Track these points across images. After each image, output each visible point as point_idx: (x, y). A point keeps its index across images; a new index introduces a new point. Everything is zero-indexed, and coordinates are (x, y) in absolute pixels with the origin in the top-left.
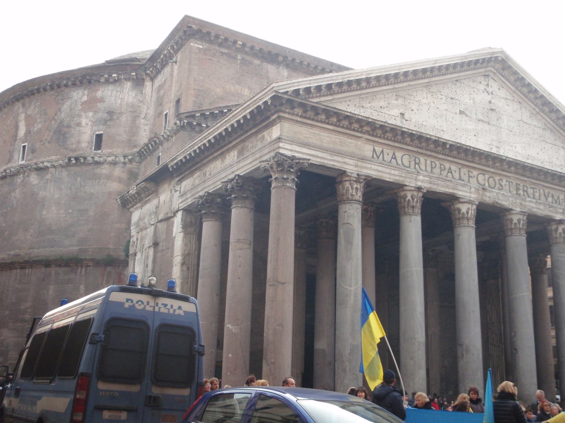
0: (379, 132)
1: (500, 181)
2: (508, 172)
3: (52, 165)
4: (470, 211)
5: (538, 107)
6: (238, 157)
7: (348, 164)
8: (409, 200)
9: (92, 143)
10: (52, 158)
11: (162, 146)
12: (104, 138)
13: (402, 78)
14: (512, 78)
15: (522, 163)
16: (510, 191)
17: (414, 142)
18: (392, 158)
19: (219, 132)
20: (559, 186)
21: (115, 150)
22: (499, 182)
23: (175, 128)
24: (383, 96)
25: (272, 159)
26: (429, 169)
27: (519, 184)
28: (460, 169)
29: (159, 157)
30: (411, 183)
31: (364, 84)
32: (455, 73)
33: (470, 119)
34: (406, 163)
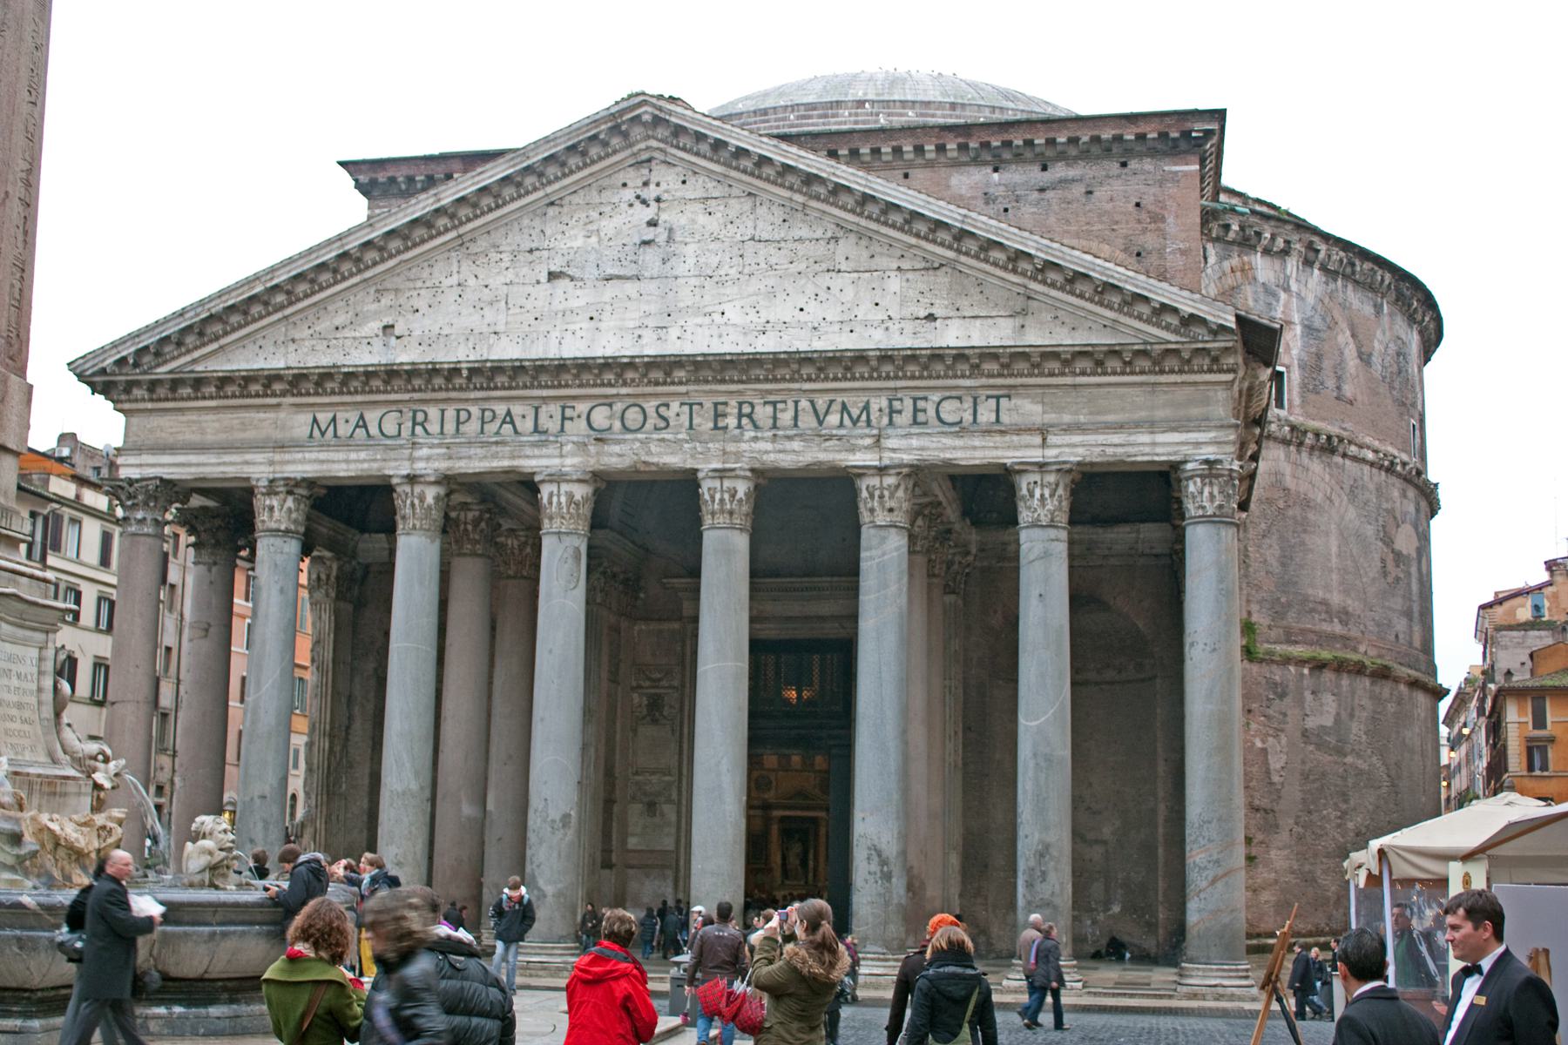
1: (662, 410)
2: (673, 383)
4: (555, 499)
5: (800, 192)
7: (254, 464)
14: (704, 148)
16: (691, 427)
18: (357, 426)
20: (854, 379)
22: (657, 412)
24: (342, 304)
26: (450, 427)
27: (726, 404)
28: (537, 409)
30: (397, 469)
32: (528, 193)
33: (581, 283)
34: (390, 427)
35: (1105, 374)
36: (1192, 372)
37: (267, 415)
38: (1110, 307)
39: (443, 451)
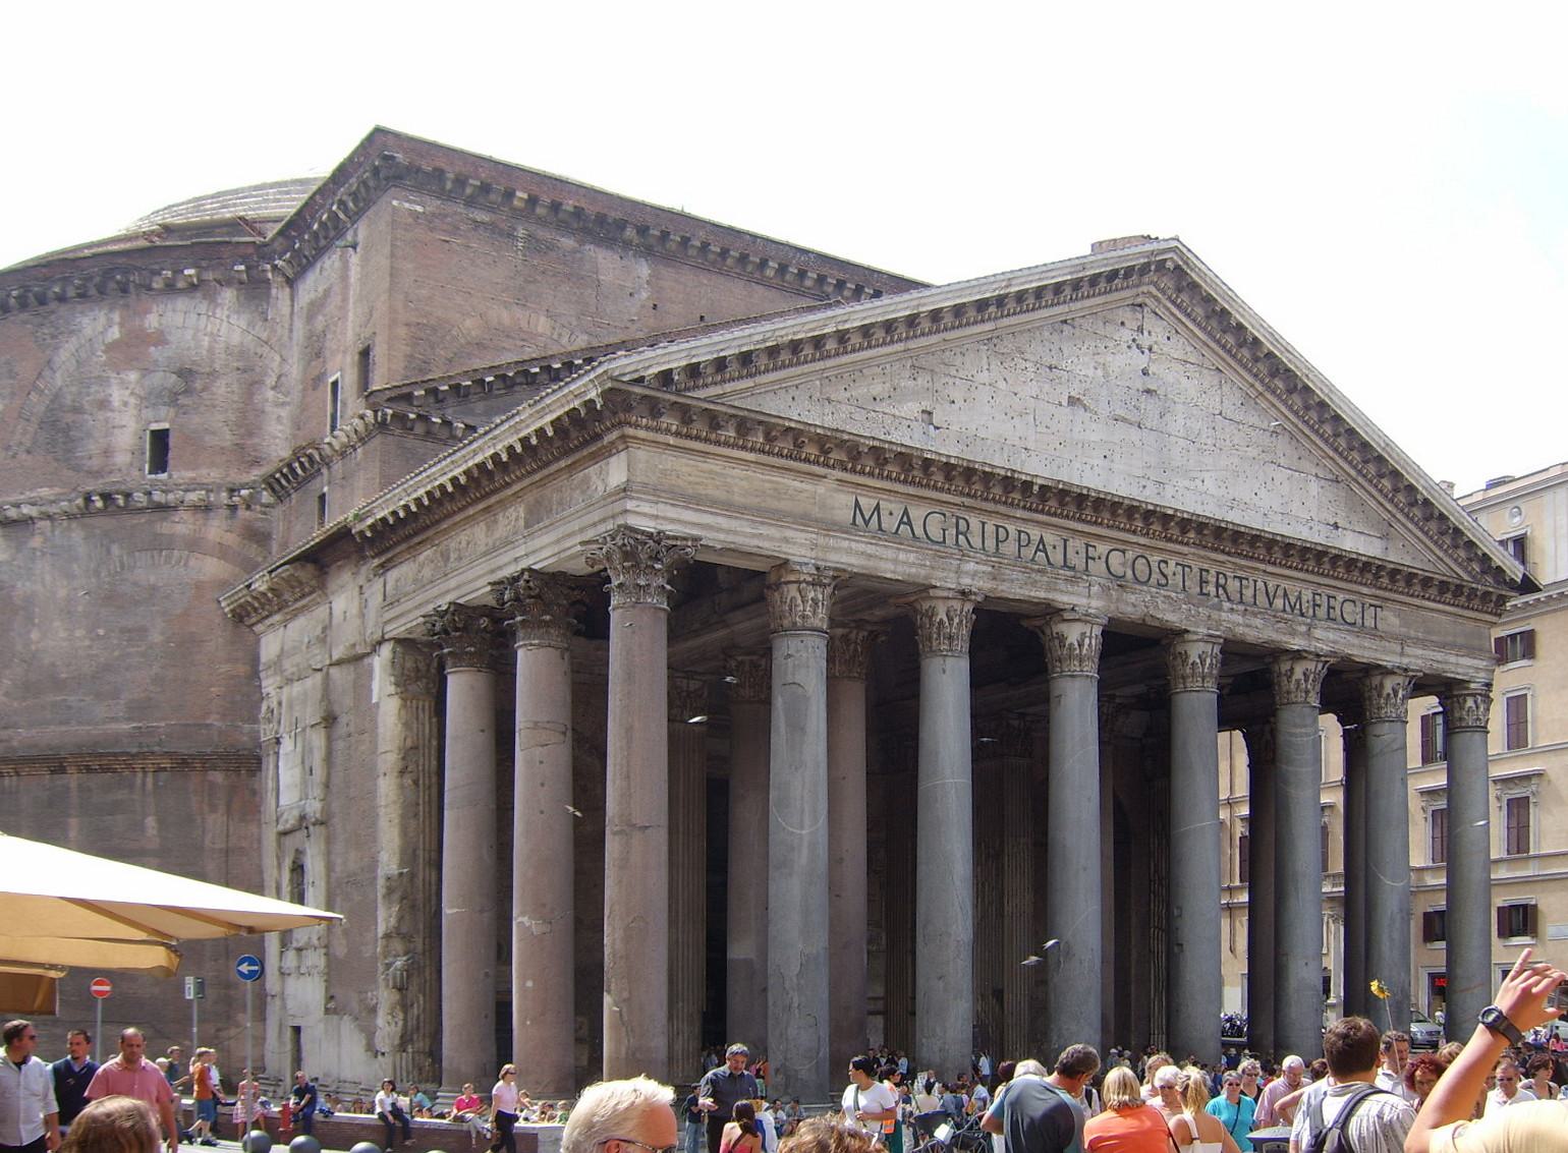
0: (869, 463)
1: (1163, 565)
2: (1181, 543)
3: (42, 513)
4: (1087, 641)
6: (527, 526)
7: (795, 543)
8: (941, 620)
9: (144, 453)
10: (42, 494)
11: (329, 468)
12: (172, 441)
13: (926, 325)
15: (1212, 521)
17: (954, 482)
18: (901, 522)
19: (479, 459)
20: (1301, 570)
21: (204, 471)
23: (361, 428)
25: (608, 539)
26: (990, 544)
27: (1207, 571)
28: (1065, 541)
29: (322, 498)
30: (946, 579)
31: (831, 345)
34: (935, 533)
35: (1439, 602)
36: (1481, 611)
37: (804, 486)
38: (1441, 547)
39: (990, 569)
